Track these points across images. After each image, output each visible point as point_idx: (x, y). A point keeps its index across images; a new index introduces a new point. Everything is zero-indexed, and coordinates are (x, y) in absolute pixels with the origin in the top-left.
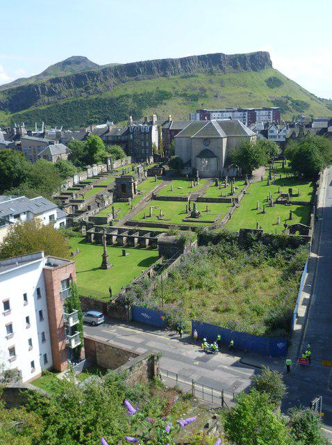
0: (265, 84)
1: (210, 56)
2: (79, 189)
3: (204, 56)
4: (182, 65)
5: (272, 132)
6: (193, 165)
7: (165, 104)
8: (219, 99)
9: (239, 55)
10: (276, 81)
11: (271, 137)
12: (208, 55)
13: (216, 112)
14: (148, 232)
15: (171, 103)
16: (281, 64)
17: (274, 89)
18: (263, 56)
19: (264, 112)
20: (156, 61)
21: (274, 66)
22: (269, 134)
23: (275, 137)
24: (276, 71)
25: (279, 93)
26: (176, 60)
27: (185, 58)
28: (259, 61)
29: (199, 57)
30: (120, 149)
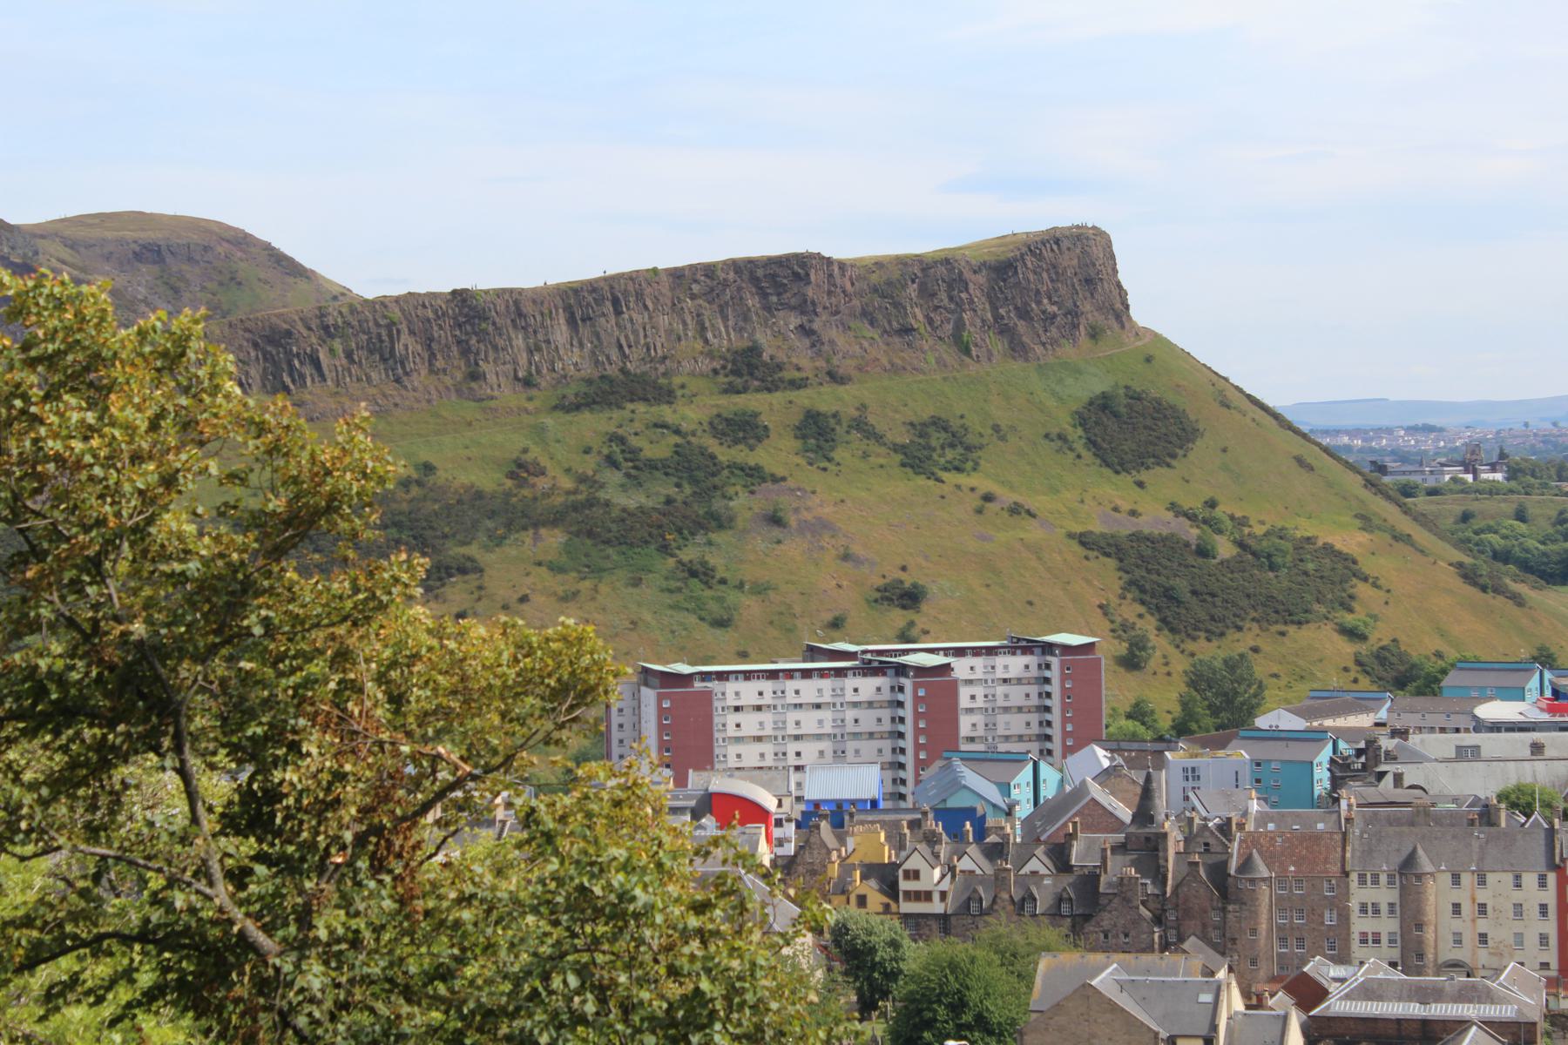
0: (1076, 435)
1: (747, 269)
3: (709, 270)
4: (572, 322)
5: (915, 875)
8: (794, 548)
9: (919, 259)
10: (1150, 416)
11: (909, 895)
12: (736, 266)
13: (748, 675)
16: (1175, 298)
18: (1069, 261)
21: (1141, 314)
22: (904, 885)
23: (927, 896)
24: (1157, 352)
27: (592, 287)
29: (677, 274)
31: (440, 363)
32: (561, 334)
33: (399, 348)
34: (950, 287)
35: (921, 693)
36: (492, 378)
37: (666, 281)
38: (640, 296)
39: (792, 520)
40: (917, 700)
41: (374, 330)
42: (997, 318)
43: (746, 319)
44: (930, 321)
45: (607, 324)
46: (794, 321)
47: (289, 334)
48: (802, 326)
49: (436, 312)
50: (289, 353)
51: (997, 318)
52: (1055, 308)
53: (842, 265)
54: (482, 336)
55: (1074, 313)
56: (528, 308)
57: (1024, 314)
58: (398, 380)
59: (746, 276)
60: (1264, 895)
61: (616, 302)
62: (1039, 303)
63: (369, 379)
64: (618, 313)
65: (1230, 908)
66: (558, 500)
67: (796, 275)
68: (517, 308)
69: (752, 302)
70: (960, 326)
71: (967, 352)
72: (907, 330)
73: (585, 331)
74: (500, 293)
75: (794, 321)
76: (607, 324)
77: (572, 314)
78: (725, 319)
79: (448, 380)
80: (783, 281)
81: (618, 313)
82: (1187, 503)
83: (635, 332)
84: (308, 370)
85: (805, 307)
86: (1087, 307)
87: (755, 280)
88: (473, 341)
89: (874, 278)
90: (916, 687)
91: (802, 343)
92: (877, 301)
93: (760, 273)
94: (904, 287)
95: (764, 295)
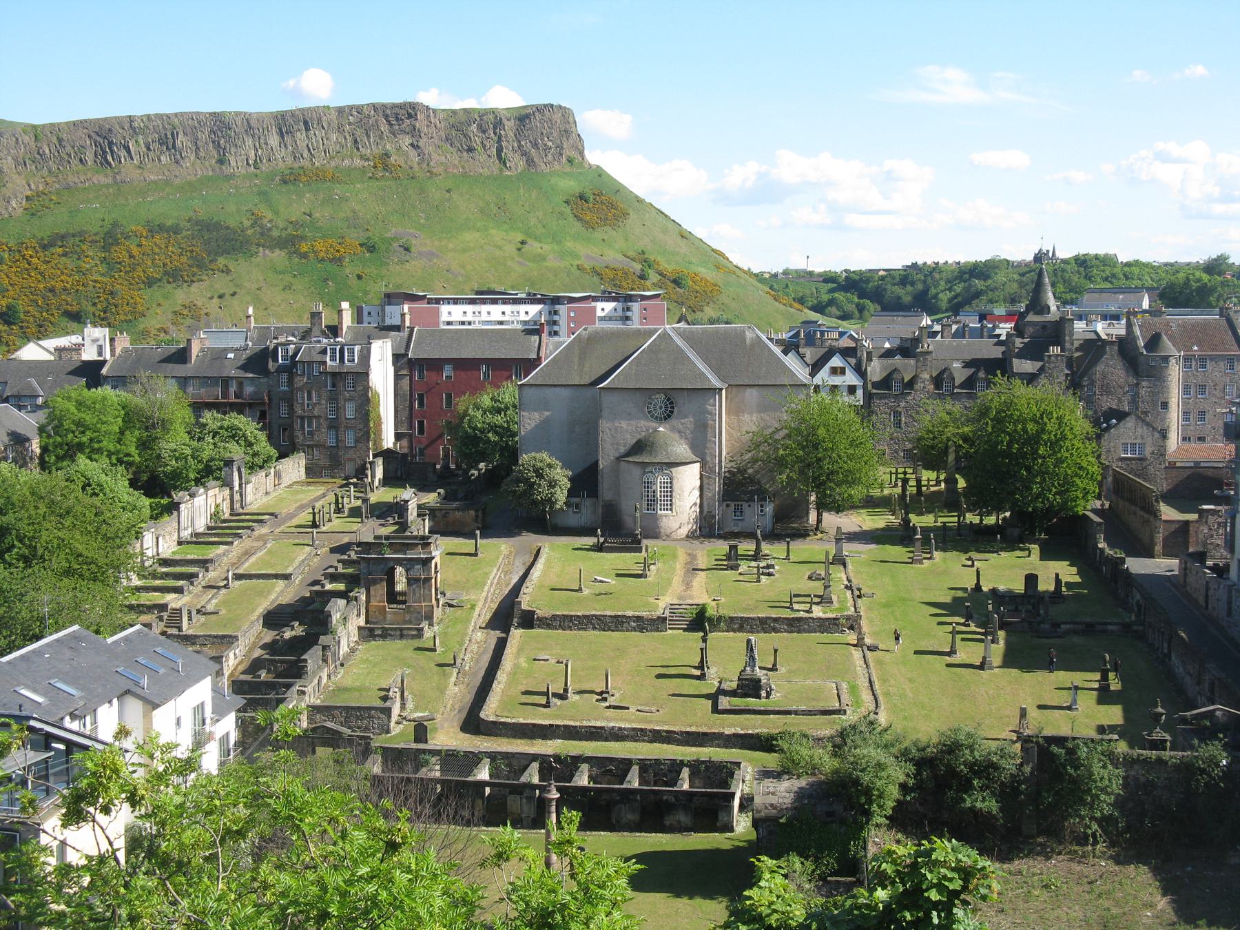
2: (179, 590)
3: (359, 109)
6: (606, 492)
7: (227, 271)
12: (374, 107)
13: (456, 301)
14: (577, 760)
15: (251, 271)
17: (599, 234)
18: (557, 117)
19: (609, 306)
20: (192, 116)
24: (599, 173)
25: (610, 249)
26: (261, 117)
27: (292, 113)
28: (539, 134)
29: (340, 111)
30: (247, 425)
31: (202, 154)
32: (274, 140)
33: (178, 143)
34: (495, 128)
35: (572, 315)
36: (233, 163)
37: (334, 116)
38: (320, 120)
39: (413, 249)
40: (570, 319)
41: (163, 132)
42: (520, 146)
43: (381, 138)
44: (484, 146)
45: (300, 136)
46: (408, 140)
47: (110, 130)
48: (412, 145)
49: (199, 123)
50: (111, 144)
51: (520, 146)
52: (550, 144)
53: (434, 111)
54: (229, 139)
55: (560, 147)
56: (253, 122)
57: (535, 145)
58: (177, 162)
59: (381, 114)
60: (1175, 374)
61: (306, 123)
62: (542, 140)
63: (160, 160)
64: (307, 129)
65: (1144, 383)
66: (275, 233)
67: (410, 116)
68: (251, 124)
69: (384, 127)
70: (499, 150)
71: (505, 164)
72: (470, 150)
73: (288, 139)
74: (237, 114)
75: (408, 140)
76: (300, 136)
77: (280, 129)
78: (368, 137)
79: (207, 163)
80: (403, 116)
81: (307, 129)
82: (630, 253)
83: (317, 141)
84: (123, 153)
85: (414, 132)
86: (565, 146)
87: (386, 117)
88: (222, 142)
89: (452, 120)
90: (570, 310)
91: (413, 153)
92: (454, 132)
93: (388, 112)
94: (469, 125)
95: (391, 125)
